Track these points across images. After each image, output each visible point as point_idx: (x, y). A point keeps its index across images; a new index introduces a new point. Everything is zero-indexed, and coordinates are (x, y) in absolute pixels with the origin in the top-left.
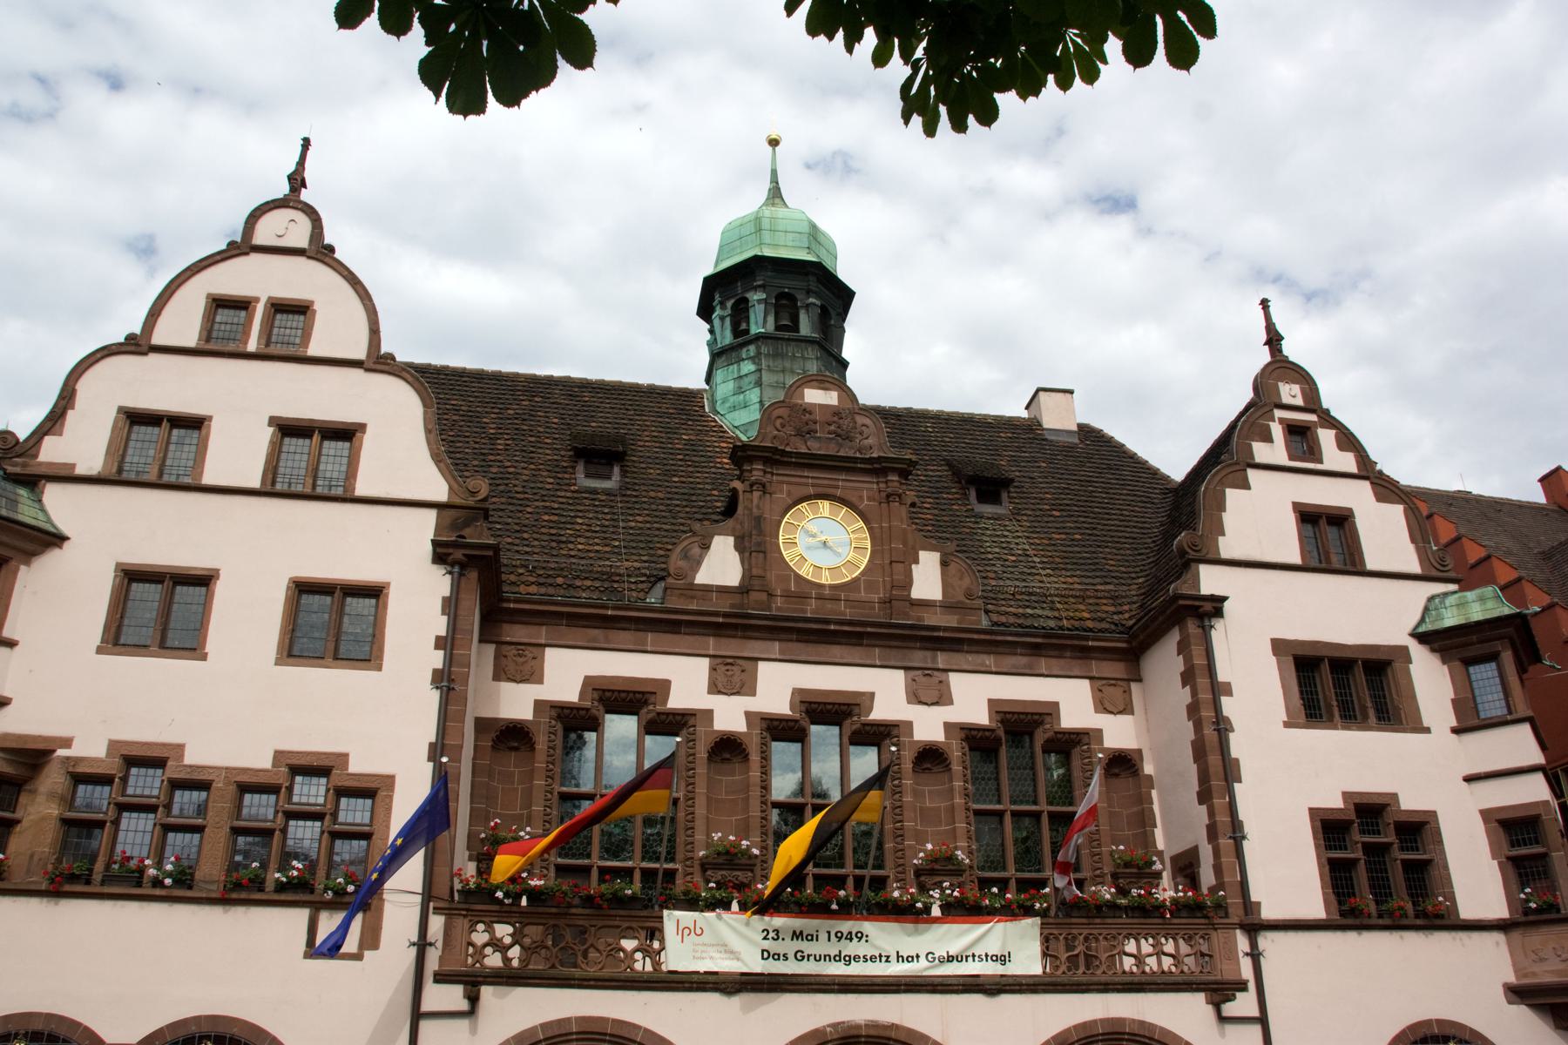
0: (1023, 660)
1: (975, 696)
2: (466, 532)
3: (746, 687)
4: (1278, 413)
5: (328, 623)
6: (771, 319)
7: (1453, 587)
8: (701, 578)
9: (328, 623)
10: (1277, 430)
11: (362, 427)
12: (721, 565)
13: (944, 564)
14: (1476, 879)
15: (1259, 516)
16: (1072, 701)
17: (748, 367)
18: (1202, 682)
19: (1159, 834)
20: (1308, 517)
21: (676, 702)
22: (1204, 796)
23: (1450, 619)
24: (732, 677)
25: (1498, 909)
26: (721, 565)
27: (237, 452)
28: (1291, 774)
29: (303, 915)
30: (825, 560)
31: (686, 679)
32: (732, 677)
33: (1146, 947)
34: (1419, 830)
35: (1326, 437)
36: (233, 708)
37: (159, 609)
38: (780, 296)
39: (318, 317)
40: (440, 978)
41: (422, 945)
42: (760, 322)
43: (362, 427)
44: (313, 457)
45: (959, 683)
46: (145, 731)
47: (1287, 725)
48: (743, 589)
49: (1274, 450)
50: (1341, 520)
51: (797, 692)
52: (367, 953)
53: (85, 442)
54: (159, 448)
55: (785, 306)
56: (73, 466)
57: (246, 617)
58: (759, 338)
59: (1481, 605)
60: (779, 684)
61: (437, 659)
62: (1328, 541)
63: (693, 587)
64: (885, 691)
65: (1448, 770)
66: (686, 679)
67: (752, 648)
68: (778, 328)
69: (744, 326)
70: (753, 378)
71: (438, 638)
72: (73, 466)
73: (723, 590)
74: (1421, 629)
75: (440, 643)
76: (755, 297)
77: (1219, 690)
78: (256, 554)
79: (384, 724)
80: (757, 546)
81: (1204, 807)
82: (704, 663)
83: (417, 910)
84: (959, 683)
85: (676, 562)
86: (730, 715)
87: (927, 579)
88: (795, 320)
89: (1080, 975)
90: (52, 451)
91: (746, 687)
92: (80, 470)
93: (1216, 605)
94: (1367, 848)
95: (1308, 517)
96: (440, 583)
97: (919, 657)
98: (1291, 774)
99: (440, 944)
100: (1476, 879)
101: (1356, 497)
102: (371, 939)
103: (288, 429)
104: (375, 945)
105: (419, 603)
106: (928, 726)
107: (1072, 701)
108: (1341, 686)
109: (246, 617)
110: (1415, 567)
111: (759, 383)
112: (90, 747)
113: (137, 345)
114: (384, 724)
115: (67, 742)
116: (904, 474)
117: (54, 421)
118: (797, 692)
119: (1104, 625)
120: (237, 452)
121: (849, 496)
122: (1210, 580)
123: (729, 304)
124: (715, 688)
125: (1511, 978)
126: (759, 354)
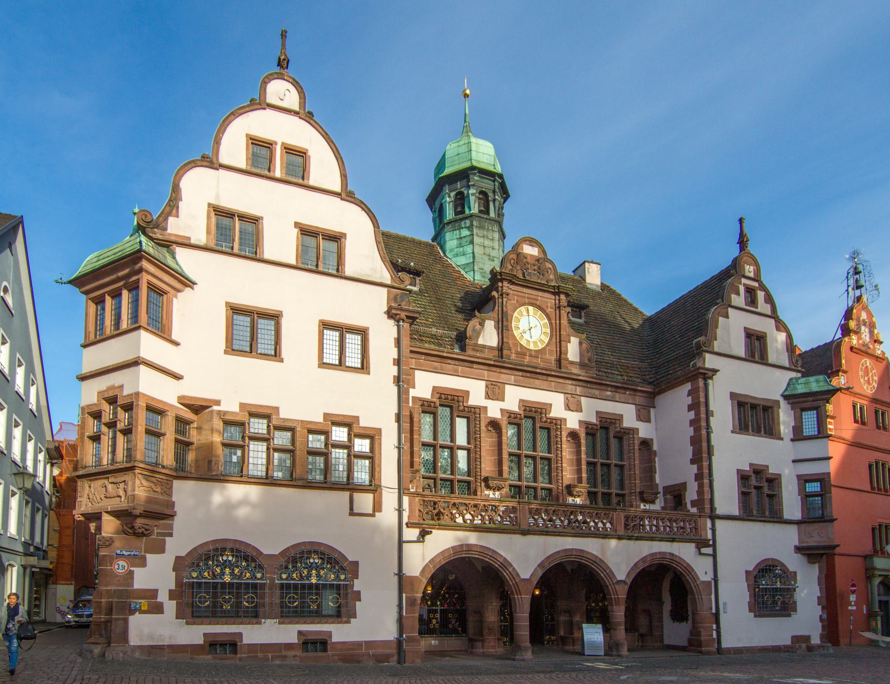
7: (799, 375)
18: (703, 409)
19: (657, 476)
22: (696, 459)
25: (797, 515)
28: (734, 452)
34: (774, 481)
36: (298, 388)
41: (400, 511)
47: (732, 432)
52: (377, 514)
57: (299, 336)
62: (756, 347)
71: (394, 359)
74: (787, 393)
77: (709, 414)
79: (372, 400)
81: (695, 466)
83: (396, 495)
99: (407, 510)
102: (377, 506)
104: (380, 510)
110: (786, 364)
114: (372, 400)
125: (797, 544)
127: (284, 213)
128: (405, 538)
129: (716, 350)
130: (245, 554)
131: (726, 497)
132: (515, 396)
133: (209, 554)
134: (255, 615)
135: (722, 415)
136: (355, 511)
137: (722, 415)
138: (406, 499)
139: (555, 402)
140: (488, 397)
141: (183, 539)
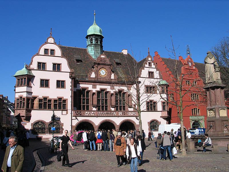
0: (122, 85)
1: (117, 88)
2: (72, 75)
3: (95, 88)
4: (148, 61)
5: (60, 84)
6: (95, 42)
8: (91, 77)
9: (60, 84)
10: (148, 63)
11: (61, 64)
12: (93, 75)
13: (114, 75)
14: (159, 107)
15: (145, 73)
16: (125, 88)
17: (93, 48)
20: (149, 73)
21: (89, 89)
23: (161, 83)
24: (94, 87)
26: (93, 75)
27: (49, 67)
28: (144, 98)
29: (61, 111)
30: (103, 74)
31: (90, 87)
32: (94, 87)
33: (131, 113)
35: (152, 64)
37: (45, 83)
38: (96, 39)
39: (56, 51)
40: (73, 116)
42: (94, 42)
43: (61, 64)
44: (57, 67)
45: (115, 87)
46: (45, 95)
48: (95, 78)
49: (147, 66)
50: (152, 73)
51: (100, 88)
53: (34, 66)
54: (42, 66)
55: (96, 40)
56: (34, 68)
57: (53, 84)
58: (94, 44)
59: (164, 82)
60: (99, 87)
61: (71, 88)
63: (90, 78)
64: (108, 88)
65: (158, 98)
66: (90, 87)
67: (96, 84)
68: (96, 43)
69: (92, 42)
70: (93, 49)
72: (34, 68)
73: (93, 78)
75: (71, 86)
76: (93, 39)
78: (53, 77)
80: (97, 73)
82: (92, 86)
84: (115, 87)
85: (88, 75)
86: (94, 91)
87: (113, 77)
88: (98, 42)
89: (125, 116)
90: (32, 67)
91: (95, 88)
92: (35, 69)
93: (140, 82)
94: (150, 104)
95: (149, 73)
96: (70, 80)
97: (111, 85)
98: (144, 98)
100: (159, 107)
101: (154, 70)
102: (67, 113)
103: (54, 64)
105: (69, 83)
106: (112, 92)
107: (125, 88)
108: (150, 89)
109: (53, 84)
111: (94, 50)
112: (41, 97)
113: (38, 54)
115: (38, 96)
116: (111, 65)
117: (31, 64)
118: (100, 88)
119: (129, 81)
120: (49, 67)
121: (105, 68)
122: (140, 79)
123: (90, 39)
124: (93, 88)
126: (94, 46)
127: (49, 61)
128: (72, 119)
129: (141, 77)
130: (43, 122)
131: (143, 107)
132: (99, 87)
133: (37, 123)
134: (44, 133)
135: (142, 89)
136: (63, 114)
137: (142, 89)
138: (73, 111)
139: (108, 88)
140: (93, 88)
141: (33, 120)
